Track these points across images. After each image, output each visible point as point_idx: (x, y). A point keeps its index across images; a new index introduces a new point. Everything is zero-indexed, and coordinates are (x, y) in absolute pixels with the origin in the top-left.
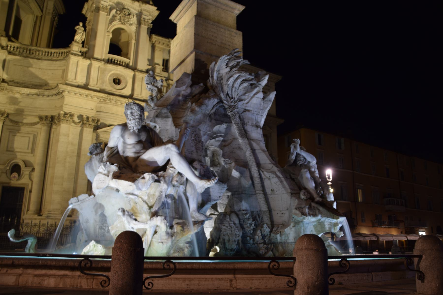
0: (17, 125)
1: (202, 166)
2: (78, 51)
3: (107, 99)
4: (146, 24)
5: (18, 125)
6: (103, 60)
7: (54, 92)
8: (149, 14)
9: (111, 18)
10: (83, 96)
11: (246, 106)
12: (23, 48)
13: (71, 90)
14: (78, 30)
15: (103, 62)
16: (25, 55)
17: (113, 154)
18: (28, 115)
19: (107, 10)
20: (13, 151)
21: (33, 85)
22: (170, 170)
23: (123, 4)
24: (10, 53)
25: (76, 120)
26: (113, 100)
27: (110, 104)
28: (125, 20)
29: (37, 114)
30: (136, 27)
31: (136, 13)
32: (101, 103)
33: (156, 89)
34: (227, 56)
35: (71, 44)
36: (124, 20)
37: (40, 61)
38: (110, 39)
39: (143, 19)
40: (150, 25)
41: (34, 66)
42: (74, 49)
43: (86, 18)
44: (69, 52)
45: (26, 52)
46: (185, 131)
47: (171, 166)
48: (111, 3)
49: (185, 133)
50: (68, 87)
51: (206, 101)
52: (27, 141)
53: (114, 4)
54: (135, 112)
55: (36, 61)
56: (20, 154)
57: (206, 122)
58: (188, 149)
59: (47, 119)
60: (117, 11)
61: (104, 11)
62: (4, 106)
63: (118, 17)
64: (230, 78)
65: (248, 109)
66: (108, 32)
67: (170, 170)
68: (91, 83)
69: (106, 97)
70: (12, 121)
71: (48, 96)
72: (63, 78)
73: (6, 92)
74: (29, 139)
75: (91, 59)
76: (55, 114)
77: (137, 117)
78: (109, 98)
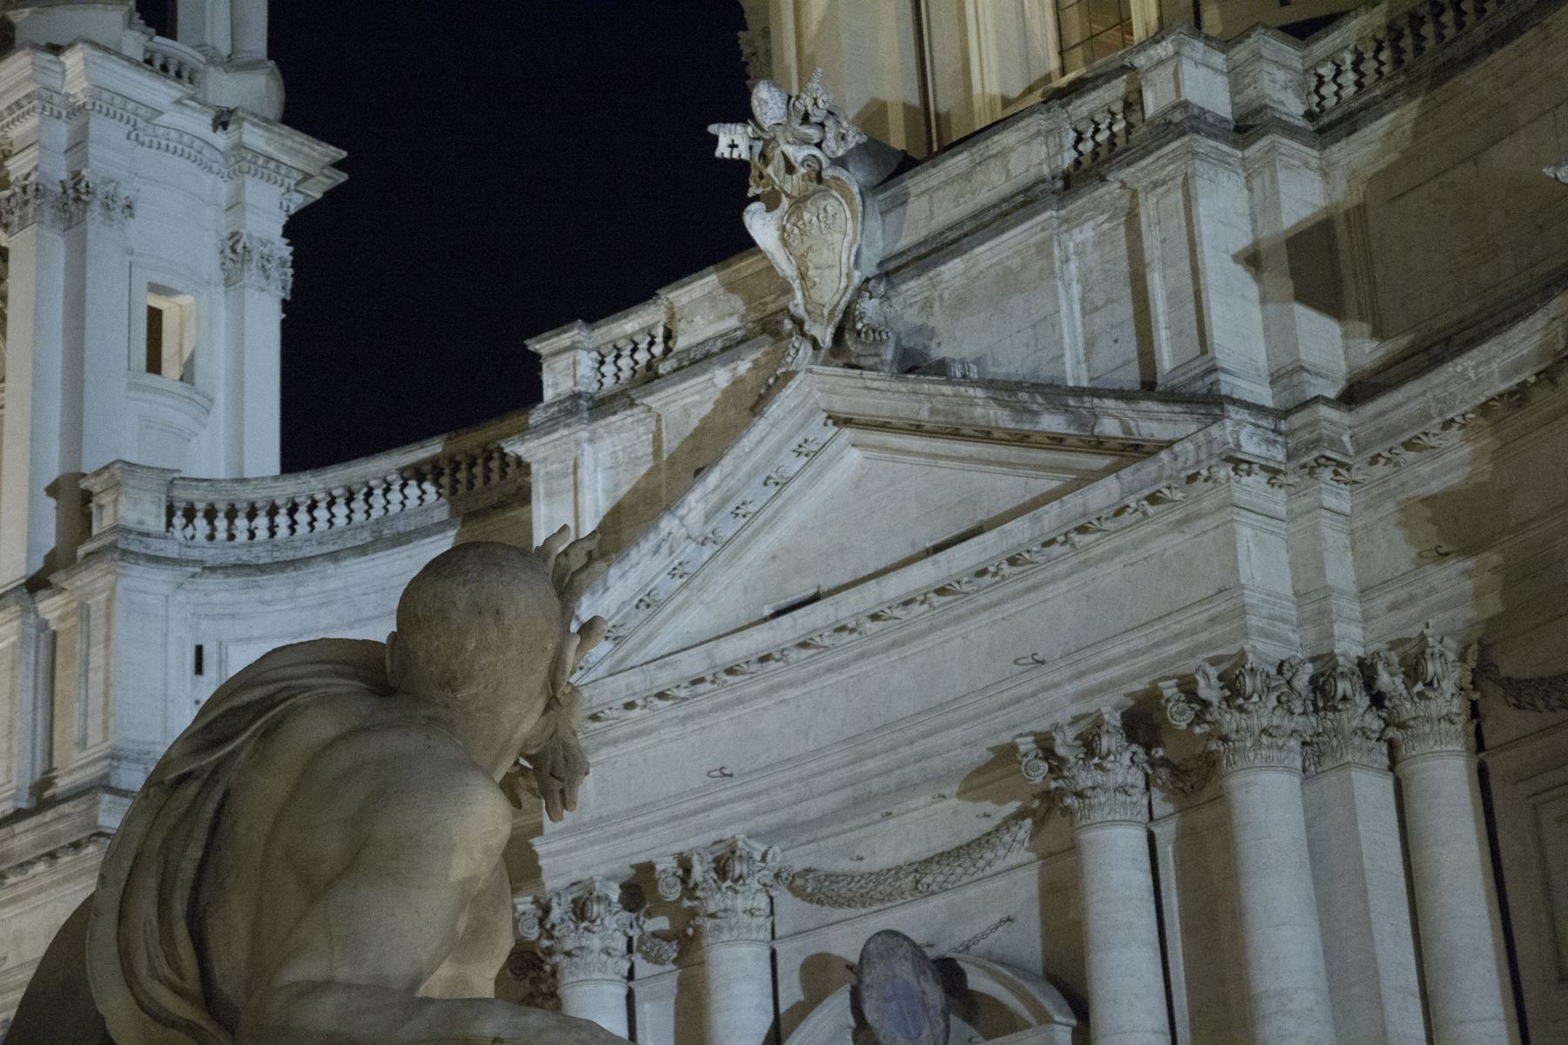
62: (1412, 600)
70: (1520, 692)
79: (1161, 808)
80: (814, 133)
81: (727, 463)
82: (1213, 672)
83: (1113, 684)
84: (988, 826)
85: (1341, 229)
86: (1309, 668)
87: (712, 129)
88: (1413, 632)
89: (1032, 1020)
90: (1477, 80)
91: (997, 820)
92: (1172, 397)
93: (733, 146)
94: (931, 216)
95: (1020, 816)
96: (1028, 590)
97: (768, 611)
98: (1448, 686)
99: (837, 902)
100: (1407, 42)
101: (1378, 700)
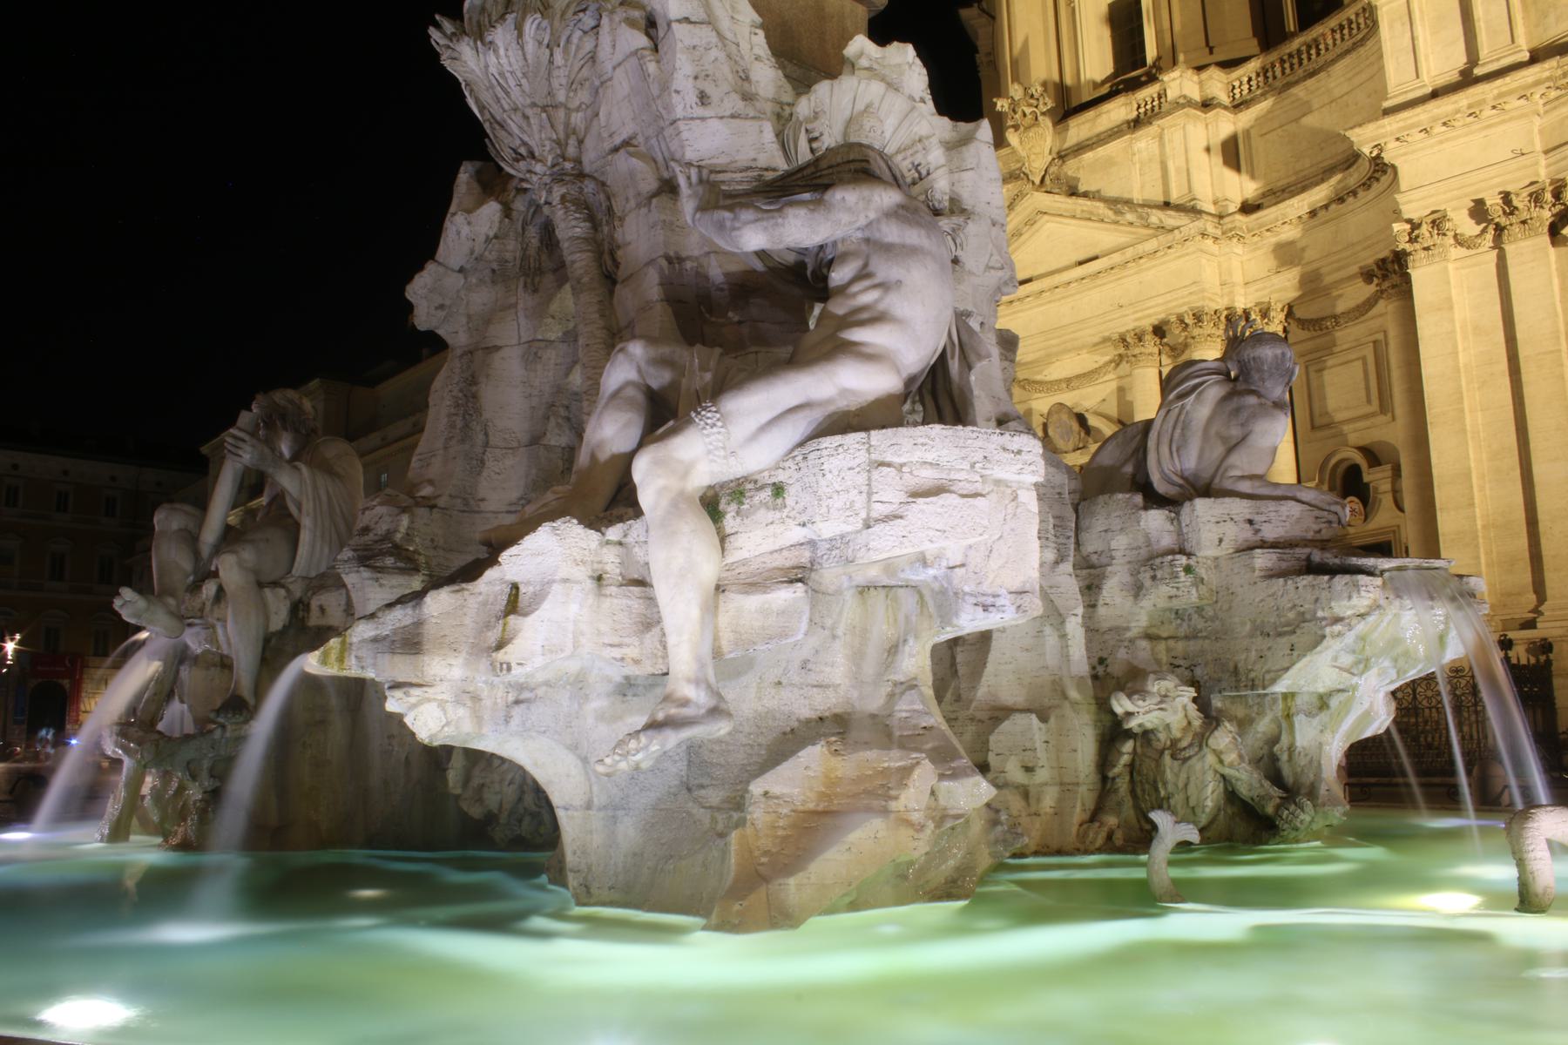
0: (1321, 330)
5: (1325, 331)
10: (1456, 124)
11: (610, 136)
16: (1278, 84)
18: (1341, 281)
20: (1328, 426)
25: (1470, 228)
29: (1355, 269)
32: (1555, 108)
37: (1322, 75)
41: (1316, 106)
50: (1384, 126)
52: (1361, 375)
55: (1310, 82)
56: (1352, 426)
57: (515, 305)
62: (1265, 288)
65: (622, 139)
68: (1484, 52)
70: (1303, 324)
74: (1365, 364)
80: (1034, 102)
83: (1149, 316)
84: (1097, 366)
86: (1225, 313)
87: (995, 100)
88: (1267, 300)
90: (1299, 91)
91: (1101, 363)
92: (1179, 208)
93: (1002, 106)
94: (1078, 135)
98: (1276, 321)
100: (1270, 74)
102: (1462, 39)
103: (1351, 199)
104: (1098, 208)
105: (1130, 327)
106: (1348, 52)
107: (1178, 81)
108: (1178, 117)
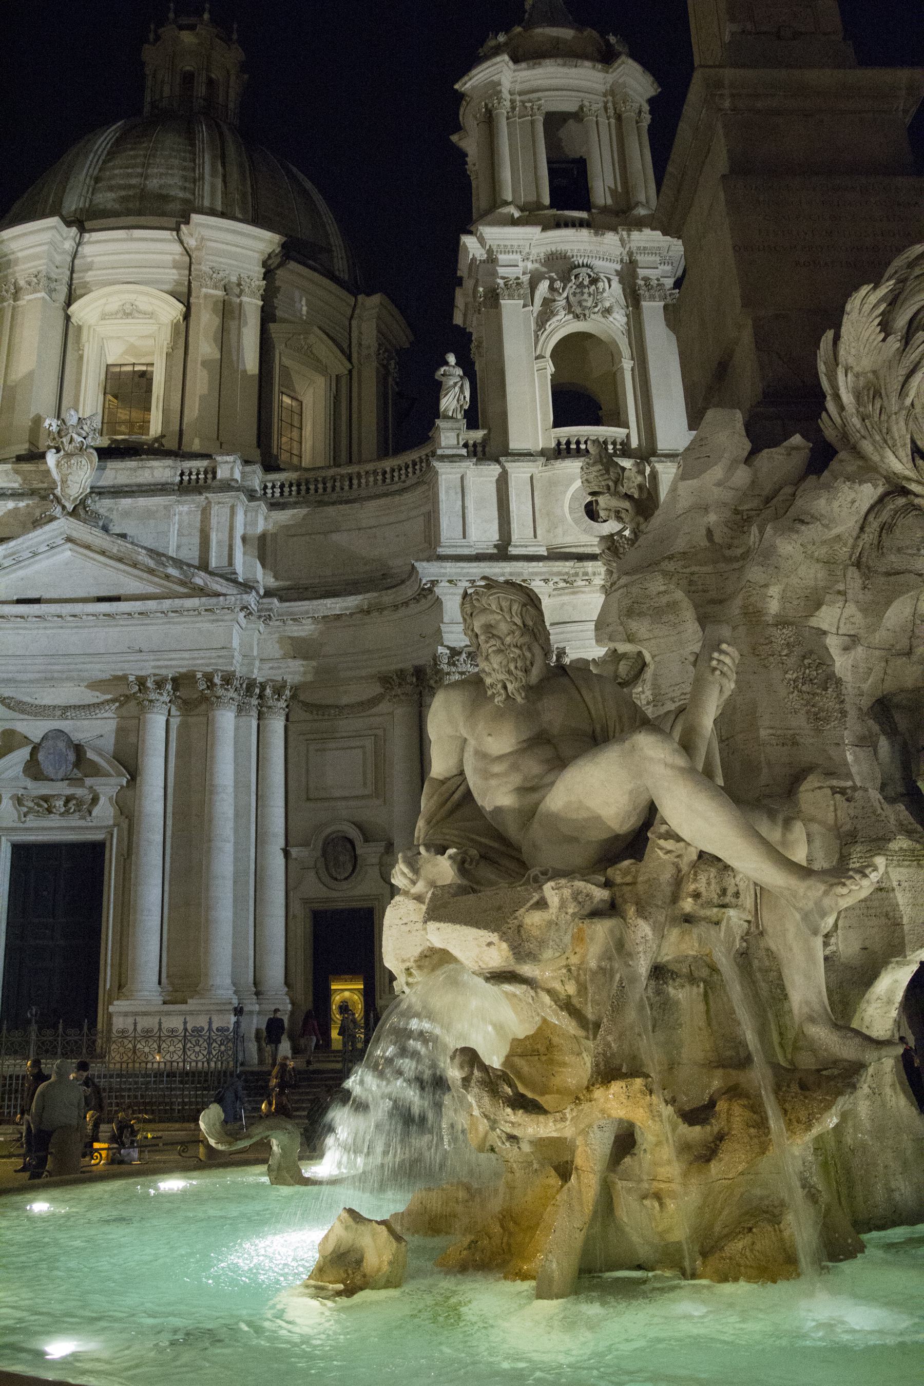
1: (838, 796)
2: (458, 444)
3: (577, 574)
4: (657, 294)
6: (543, 453)
7: (408, 591)
8: (658, 259)
9: (540, 311)
12: (307, 482)
13: (456, 574)
14: (443, 379)
15: (542, 460)
17: (449, 805)
19: (522, 291)
21: (347, 584)
22: (661, 849)
23: (569, 254)
24: (274, 506)
26: (594, 574)
27: (590, 592)
28: (584, 304)
30: (627, 316)
31: (616, 271)
32: (560, 595)
33: (627, 504)
34: (875, 288)
35: (434, 429)
36: (580, 303)
37: (356, 505)
38: (549, 377)
39: (642, 283)
40: (671, 295)
42: (443, 444)
43: (471, 334)
44: (434, 454)
45: (316, 491)
46: (712, 659)
47: (664, 828)
48: (530, 266)
49: (714, 669)
50: (445, 568)
51: (821, 504)
53: (537, 265)
54: (498, 622)
58: (772, 728)
59: (404, 679)
60: (552, 281)
61: (511, 297)
62: (279, 668)
63: (561, 302)
64: (911, 380)
66: (537, 358)
67: (661, 849)
68: (515, 537)
69: (572, 571)
70: (308, 707)
71: (396, 607)
72: (430, 544)
73: (278, 623)
75: (502, 459)
76: (423, 659)
77: (508, 640)
78: (581, 571)
79: (174, 711)
81: (20, 540)
82: (220, 674)
84: (96, 701)
85: (269, 538)
89: (112, 772)
90: (331, 511)
93: (50, 425)
94: (116, 478)
95: (113, 701)
96: (142, 625)
97: (15, 598)
99: (23, 712)
101: (261, 696)
102: (496, 522)
103: (375, 614)
104: (139, 554)
105: (150, 671)
106: (385, 495)
107: (230, 466)
108: (227, 498)
